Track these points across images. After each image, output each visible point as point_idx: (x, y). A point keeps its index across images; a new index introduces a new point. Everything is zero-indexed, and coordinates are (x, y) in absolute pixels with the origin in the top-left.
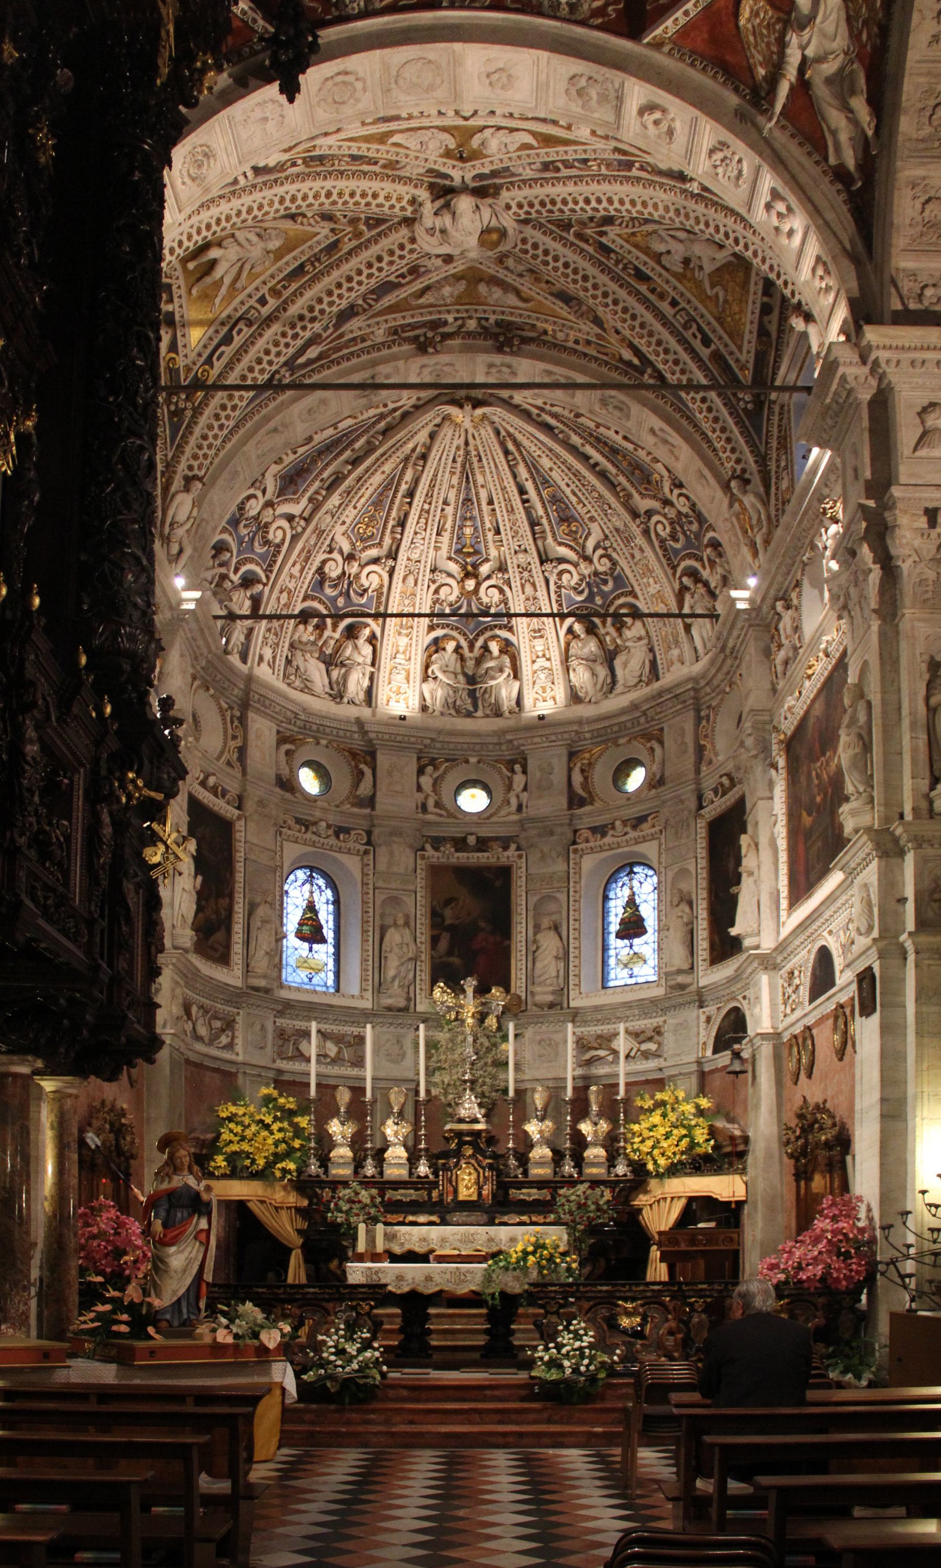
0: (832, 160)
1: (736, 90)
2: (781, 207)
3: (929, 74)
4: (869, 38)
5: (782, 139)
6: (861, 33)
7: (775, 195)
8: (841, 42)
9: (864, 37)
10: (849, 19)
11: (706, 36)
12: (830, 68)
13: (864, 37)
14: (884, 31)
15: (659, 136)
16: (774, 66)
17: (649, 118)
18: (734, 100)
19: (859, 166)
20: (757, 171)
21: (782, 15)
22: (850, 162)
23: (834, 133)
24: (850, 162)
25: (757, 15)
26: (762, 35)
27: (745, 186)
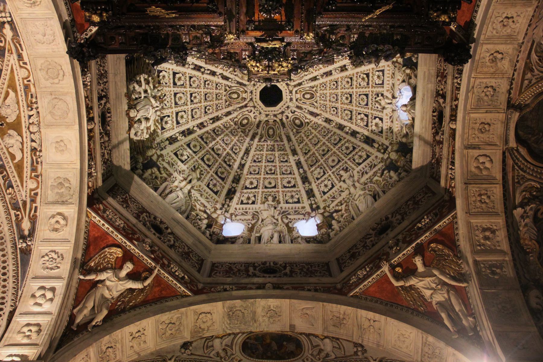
0: (75, 311)
1: (83, 255)
2: (49, 295)
3: (122, 338)
4: (120, 305)
5: (75, 284)
6: (119, 301)
7: (53, 289)
8: (116, 294)
9: (119, 303)
10: (122, 294)
11: (96, 235)
12: (107, 294)
13: (119, 303)
14: (124, 311)
15: (51, 225)
16: (96, 269)
17: (59, 218)
18: (79, 256)
19: (78, 326)
20: (59, 278)
21: (114, 265)
22: (78, 320)
23: (84, 307)
24: (78, 320)
25: (111, 255)
26: (104, 259)
27: (45, 273)
